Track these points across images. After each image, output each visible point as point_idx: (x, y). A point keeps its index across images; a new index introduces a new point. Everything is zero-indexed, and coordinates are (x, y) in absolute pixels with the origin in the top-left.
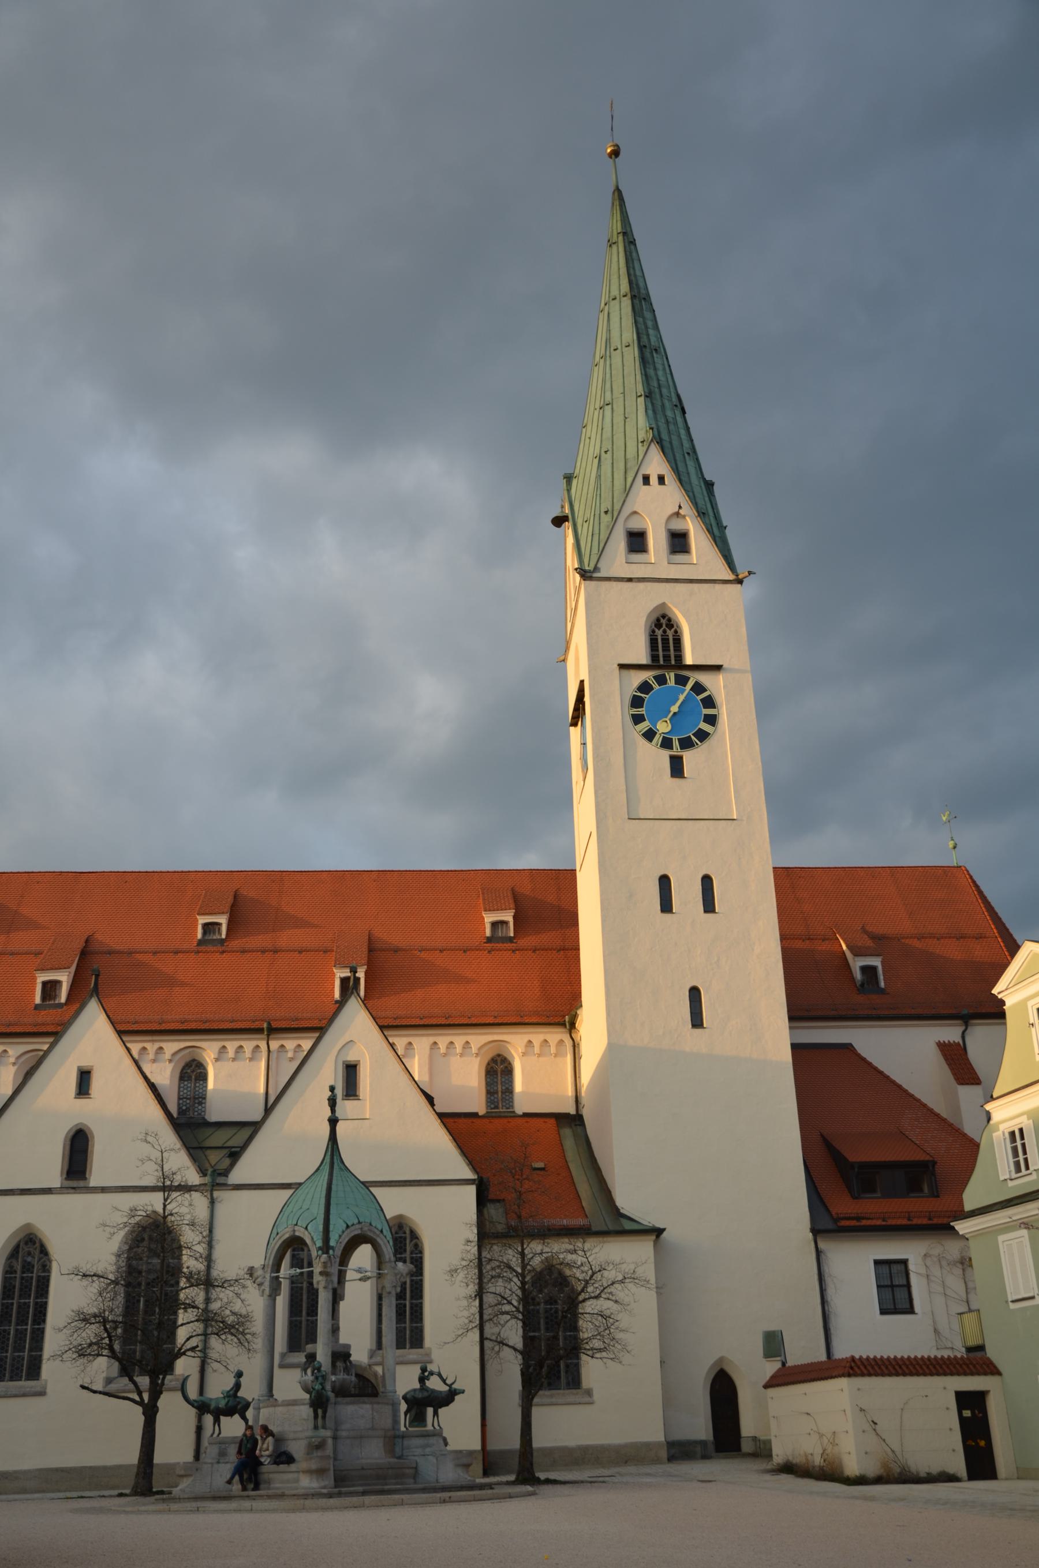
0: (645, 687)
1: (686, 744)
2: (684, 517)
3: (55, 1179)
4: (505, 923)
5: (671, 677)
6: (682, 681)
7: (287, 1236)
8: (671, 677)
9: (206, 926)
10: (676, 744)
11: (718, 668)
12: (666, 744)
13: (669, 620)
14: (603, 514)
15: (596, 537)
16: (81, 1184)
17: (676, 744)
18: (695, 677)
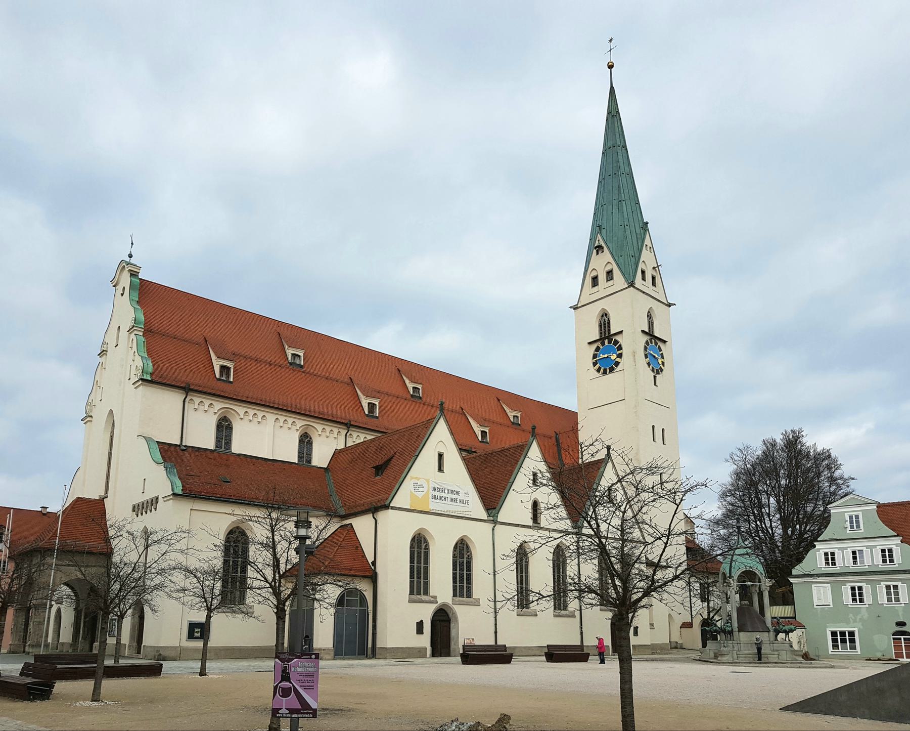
0: (647, 343)
1: (658, 373)
2: (656, 270)
3: (530, 522)
4: (517, 417)
5: (653, 341)
6: (656, 344)
7: (745, 570)
8: (653, 341)
9: (414, 388)
10: (655, 371)
11: (665, 342)
12: (653, 370)
13: (650, 314)
14: (631, 257)
15: (630, 267)
16: (538, 525)
17: (655, 371)
18: (660, 344)
